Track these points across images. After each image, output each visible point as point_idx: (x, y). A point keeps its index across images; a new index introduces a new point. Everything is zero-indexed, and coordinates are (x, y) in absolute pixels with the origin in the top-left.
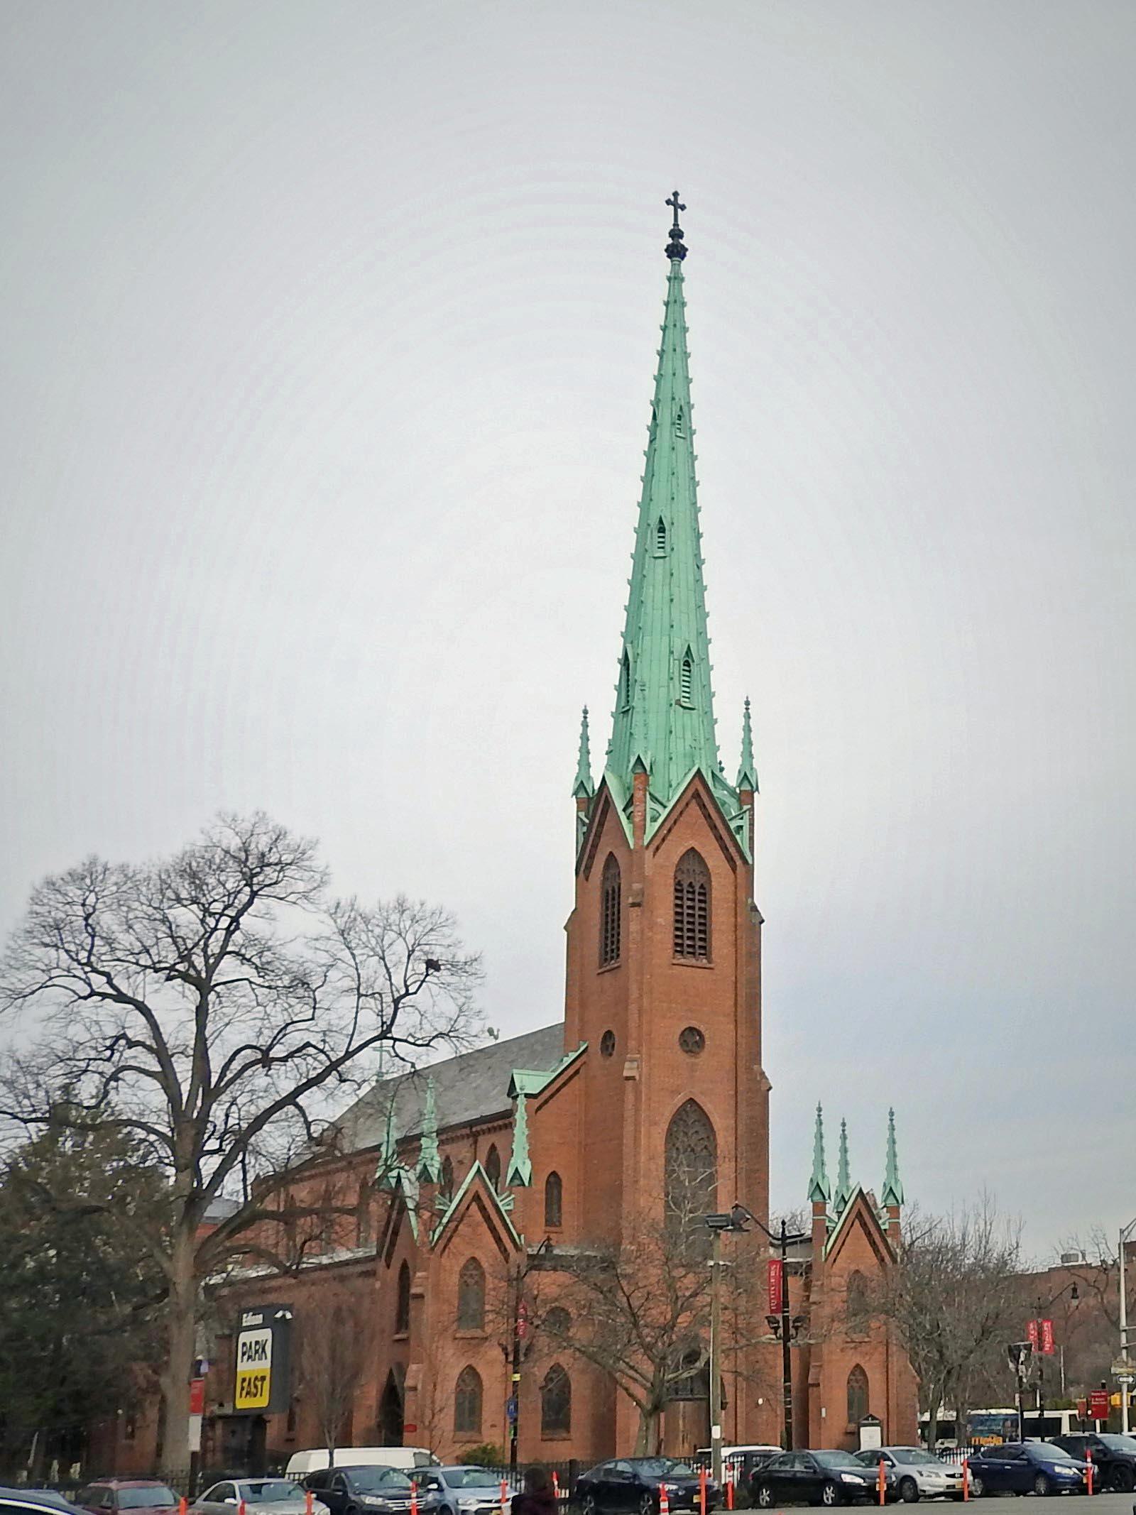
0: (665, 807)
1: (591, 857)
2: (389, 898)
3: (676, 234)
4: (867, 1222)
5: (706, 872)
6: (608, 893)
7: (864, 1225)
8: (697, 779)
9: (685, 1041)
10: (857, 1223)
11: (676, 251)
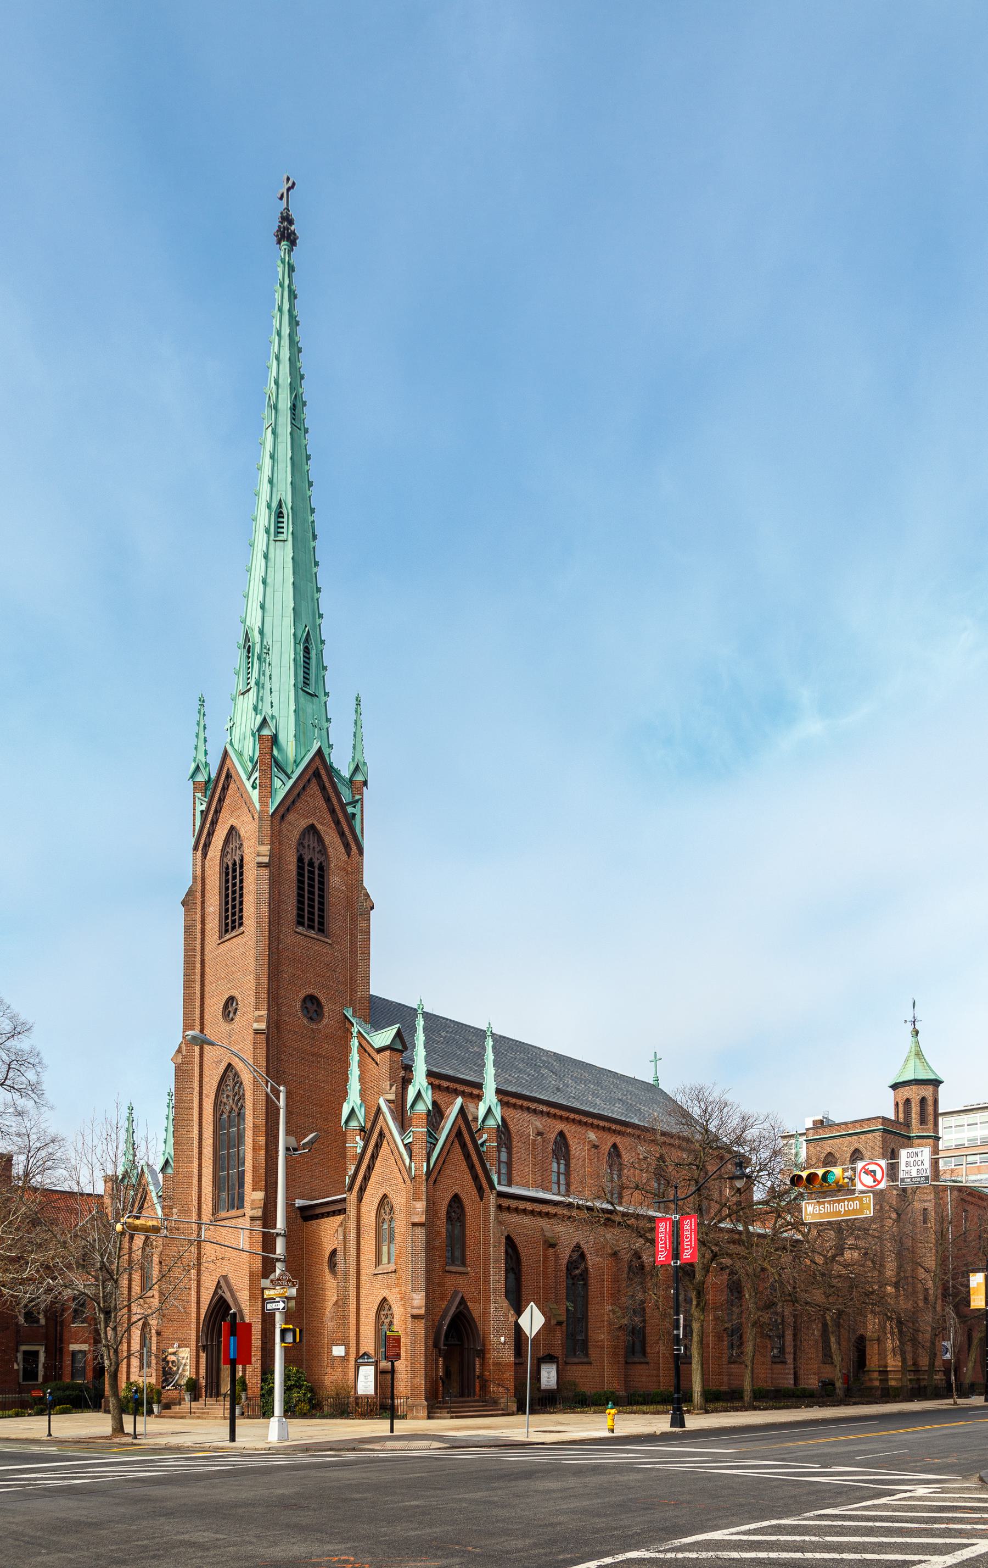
0: (289, 778)
1: (210, 834)
2: (8, 1003)
3: (286, 219)
4: (455, 1307)
5: (324, 851)
6: (227, 868)
7: (463, 1146)
8: (317, 757)
9: (306, 1007)
10: (457, 1145)
11: (287, 235)
